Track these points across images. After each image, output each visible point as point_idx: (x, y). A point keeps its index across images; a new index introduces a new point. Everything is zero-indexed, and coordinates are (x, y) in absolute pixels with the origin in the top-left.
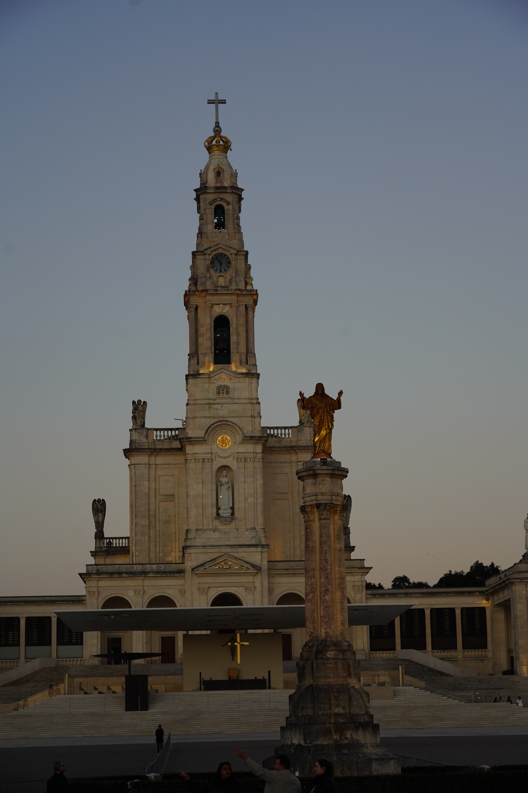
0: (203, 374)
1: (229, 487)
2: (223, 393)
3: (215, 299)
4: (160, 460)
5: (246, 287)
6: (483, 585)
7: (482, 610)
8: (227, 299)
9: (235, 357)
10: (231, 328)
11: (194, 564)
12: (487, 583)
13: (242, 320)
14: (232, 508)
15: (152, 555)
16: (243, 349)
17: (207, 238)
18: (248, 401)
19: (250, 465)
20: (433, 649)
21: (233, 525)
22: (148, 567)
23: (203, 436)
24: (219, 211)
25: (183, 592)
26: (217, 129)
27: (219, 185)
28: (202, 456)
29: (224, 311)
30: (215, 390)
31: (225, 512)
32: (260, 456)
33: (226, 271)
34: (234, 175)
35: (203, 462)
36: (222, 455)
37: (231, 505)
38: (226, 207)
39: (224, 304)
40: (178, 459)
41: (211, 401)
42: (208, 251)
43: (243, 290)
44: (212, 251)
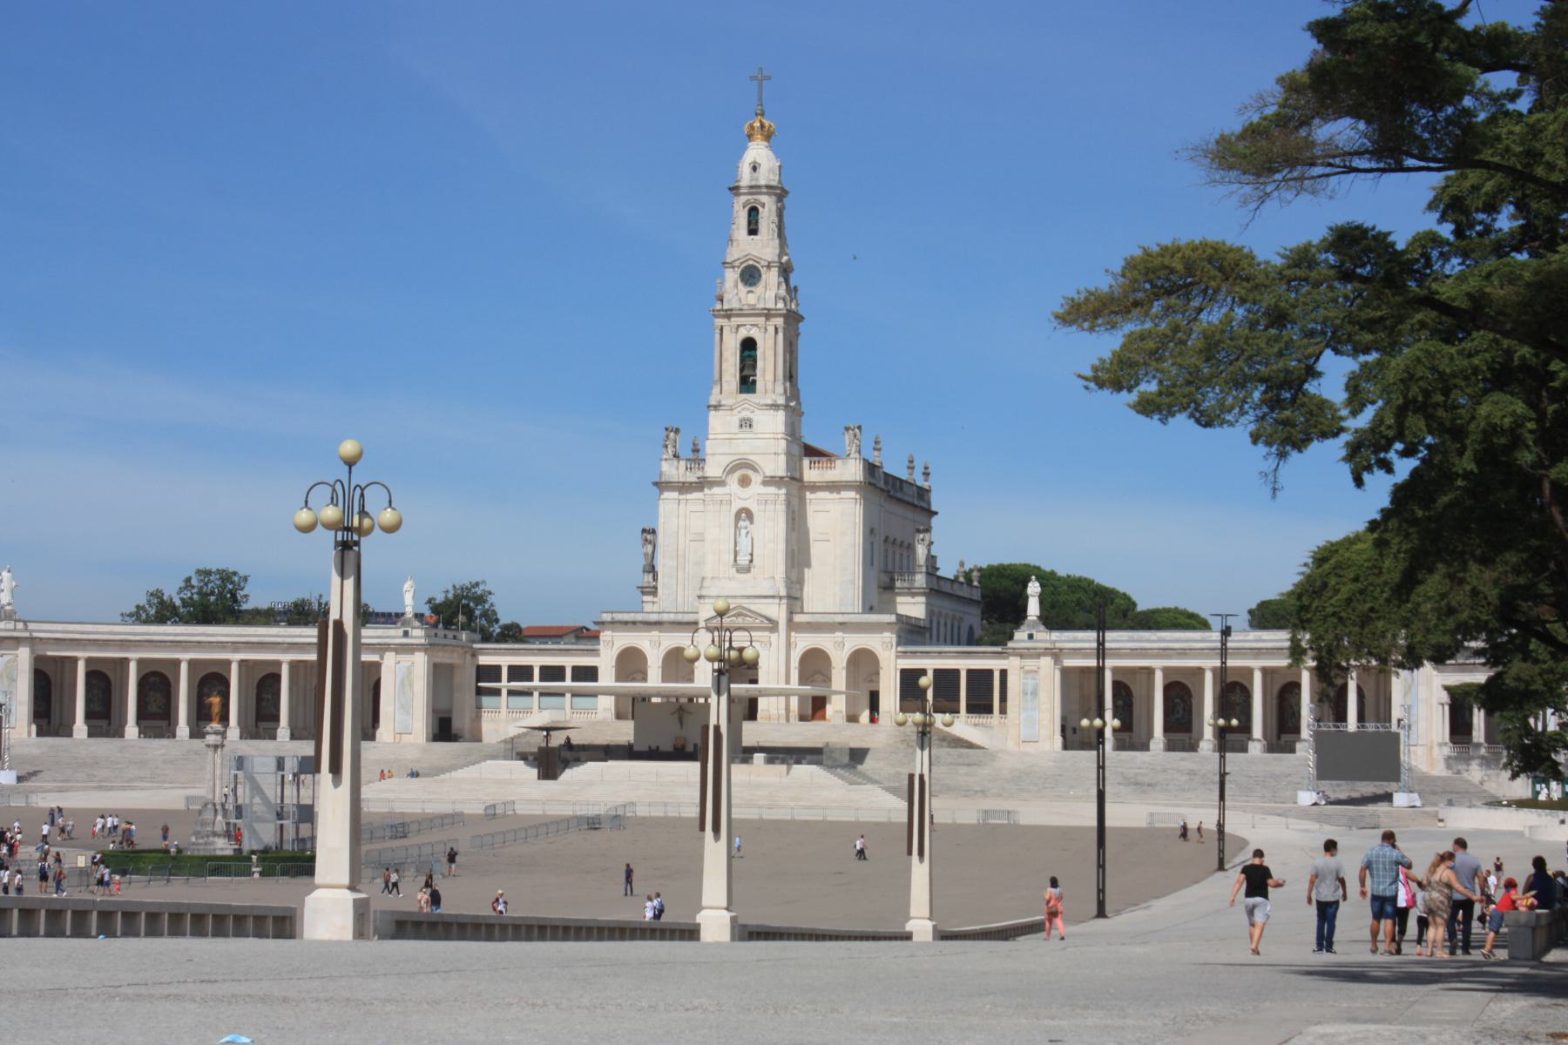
0: (724, 405)
9: (759, 386)
13: (770, 342)
14: (752, 555)
15: (680, 599)
16: (770, 377)
17: (738, 245)
18: (772, 436)
19: (770, 507)
22: (665, 617)
27: (754, 183)
28: (720, 498)
30: (737, 423)
31: (743, 559)
32: (783, 497)
37: (750, 551)
38: (760, 209)
41: (732, 436)
42: (737, 264)
44: (741, 263)
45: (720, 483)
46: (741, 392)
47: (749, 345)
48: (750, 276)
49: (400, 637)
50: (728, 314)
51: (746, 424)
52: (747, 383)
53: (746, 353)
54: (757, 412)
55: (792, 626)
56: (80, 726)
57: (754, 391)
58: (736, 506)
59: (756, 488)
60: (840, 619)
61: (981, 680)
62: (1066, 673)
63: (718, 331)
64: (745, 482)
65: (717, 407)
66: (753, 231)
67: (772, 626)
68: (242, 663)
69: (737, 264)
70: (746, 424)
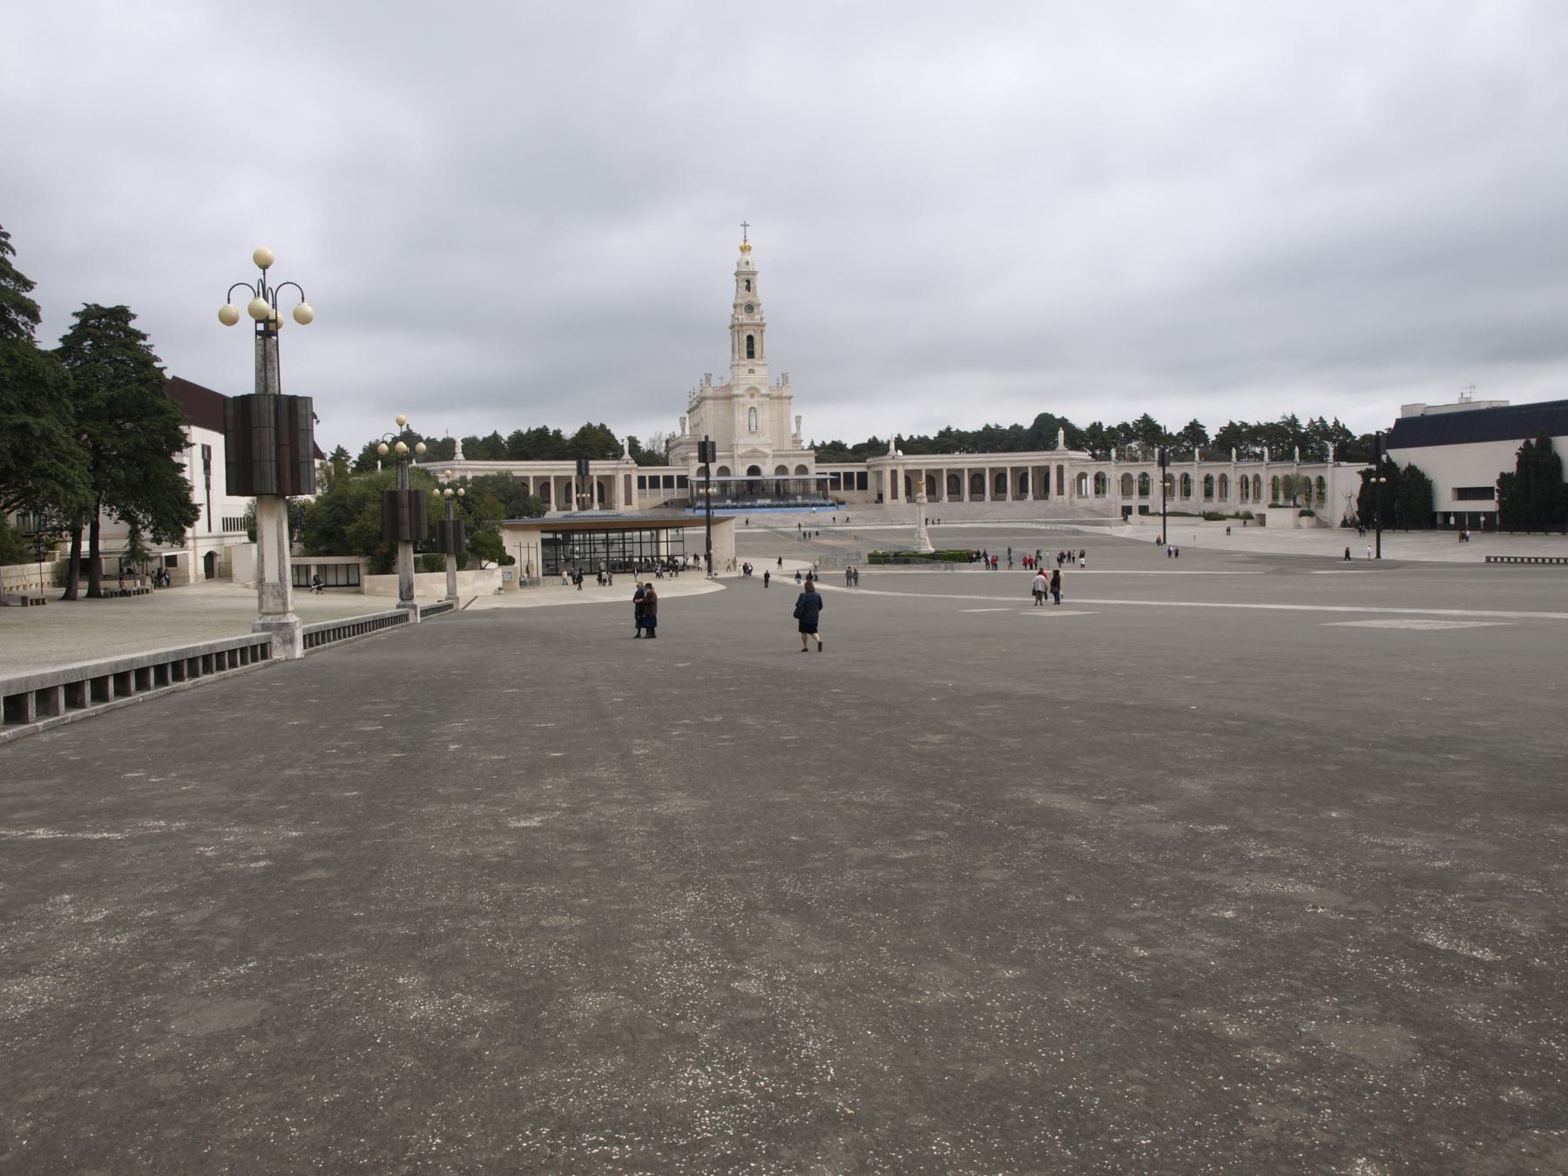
4: (718, 402)
6: (865, 462)
7: (866, 473)
8: (752, 327)
12: (868, 460)
21: (756, 435)
24: (748, 281)
25: (733, 464)
26: (745, 241)
34: (753, 265)
40: (728, 401)
45: (742, 396)
46: (748, 357)
47: (750, 338)
50: (741, 325)
52: (751, 354)
55: (774, 456)
56: (945, 497)
58: (749, 406)
60: (791, 452)
61: (1043, 474)
62: (906, 471)
64: (752, 396)
65: (738, 365)
67: (765, 456)
68: (534, 477)
70: (751, 371)
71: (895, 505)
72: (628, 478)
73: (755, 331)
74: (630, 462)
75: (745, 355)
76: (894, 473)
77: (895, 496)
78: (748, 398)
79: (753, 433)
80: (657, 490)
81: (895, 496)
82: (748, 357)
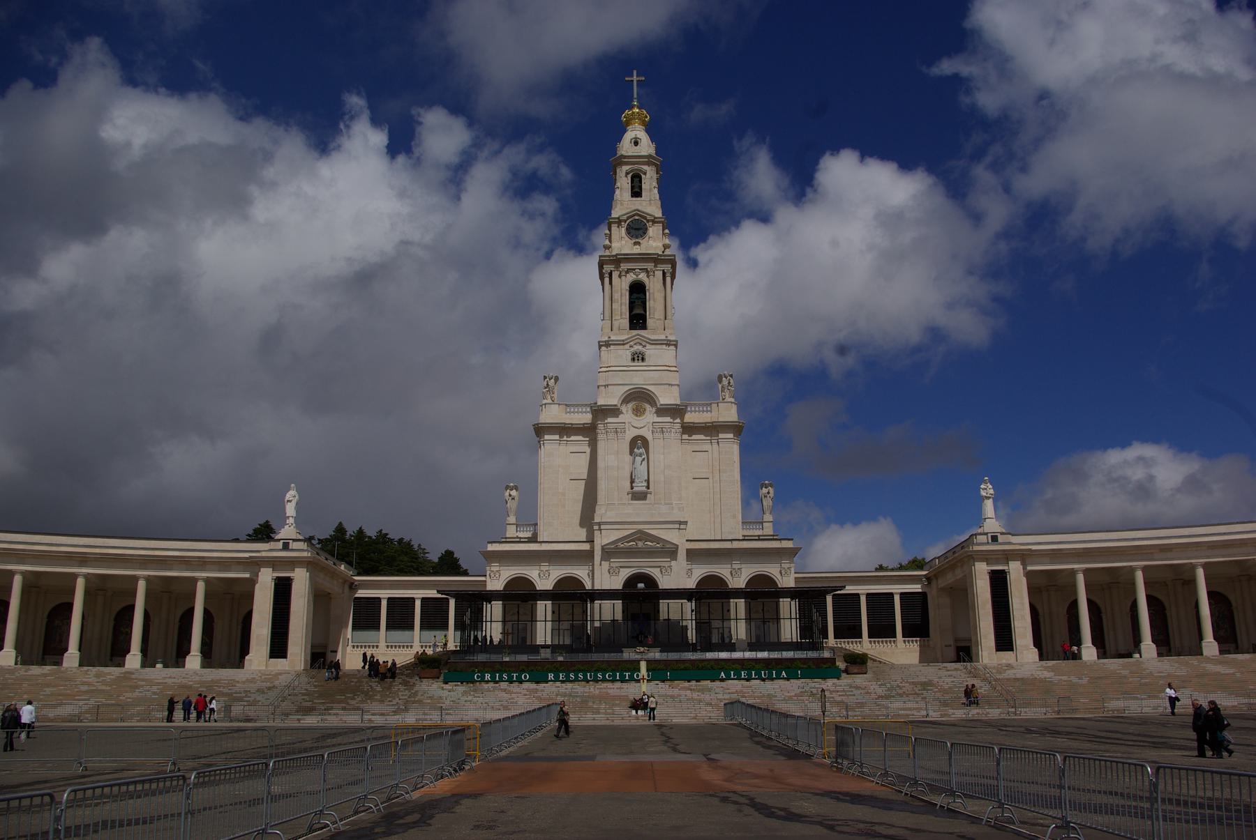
1: (644, 459)
2: (638, 360)
3: (630, 266)
5: (663, 252)
9: (650, 322)
10: (647, 294)
11: (606, 541)
14: (648, 481)
19: (666, 435)
20: (870, 637)
23: (615, 403)
25: (592, 575)
29: (640, 276)
30: (630, 357)
33: (642, 236)
35: (617, 432)
36: (634, 425)
37: (646, 478)
38: (643, 176)
39: (640, 269)
43: (661, 255)
44: (628, 218)
46: (633, 326)
47: (638, 290)
48: (637, 228)
49: (281, 550)
50: (617, 260)
51: (638, 357)
52: (638, 320)
53: (635, 296)
54: (648, 346)
57: (644, 327)
59: (650, 416)
63: (607, 275)
64: (638, 412)
66: (636, 192)
67: (671, 552)
69: (625, 217)
70: (638, 357)
71: (1009, 666)
72: (283, 589)
73: (646, 271)
74: (293, 545)
75: (626, 322)
76: (999, 582)
77: (1004, 641)
78: (627, 415)
79: (639, 496)
80: (407, 633)
81: (1004, 641)
82: (633, 326)
